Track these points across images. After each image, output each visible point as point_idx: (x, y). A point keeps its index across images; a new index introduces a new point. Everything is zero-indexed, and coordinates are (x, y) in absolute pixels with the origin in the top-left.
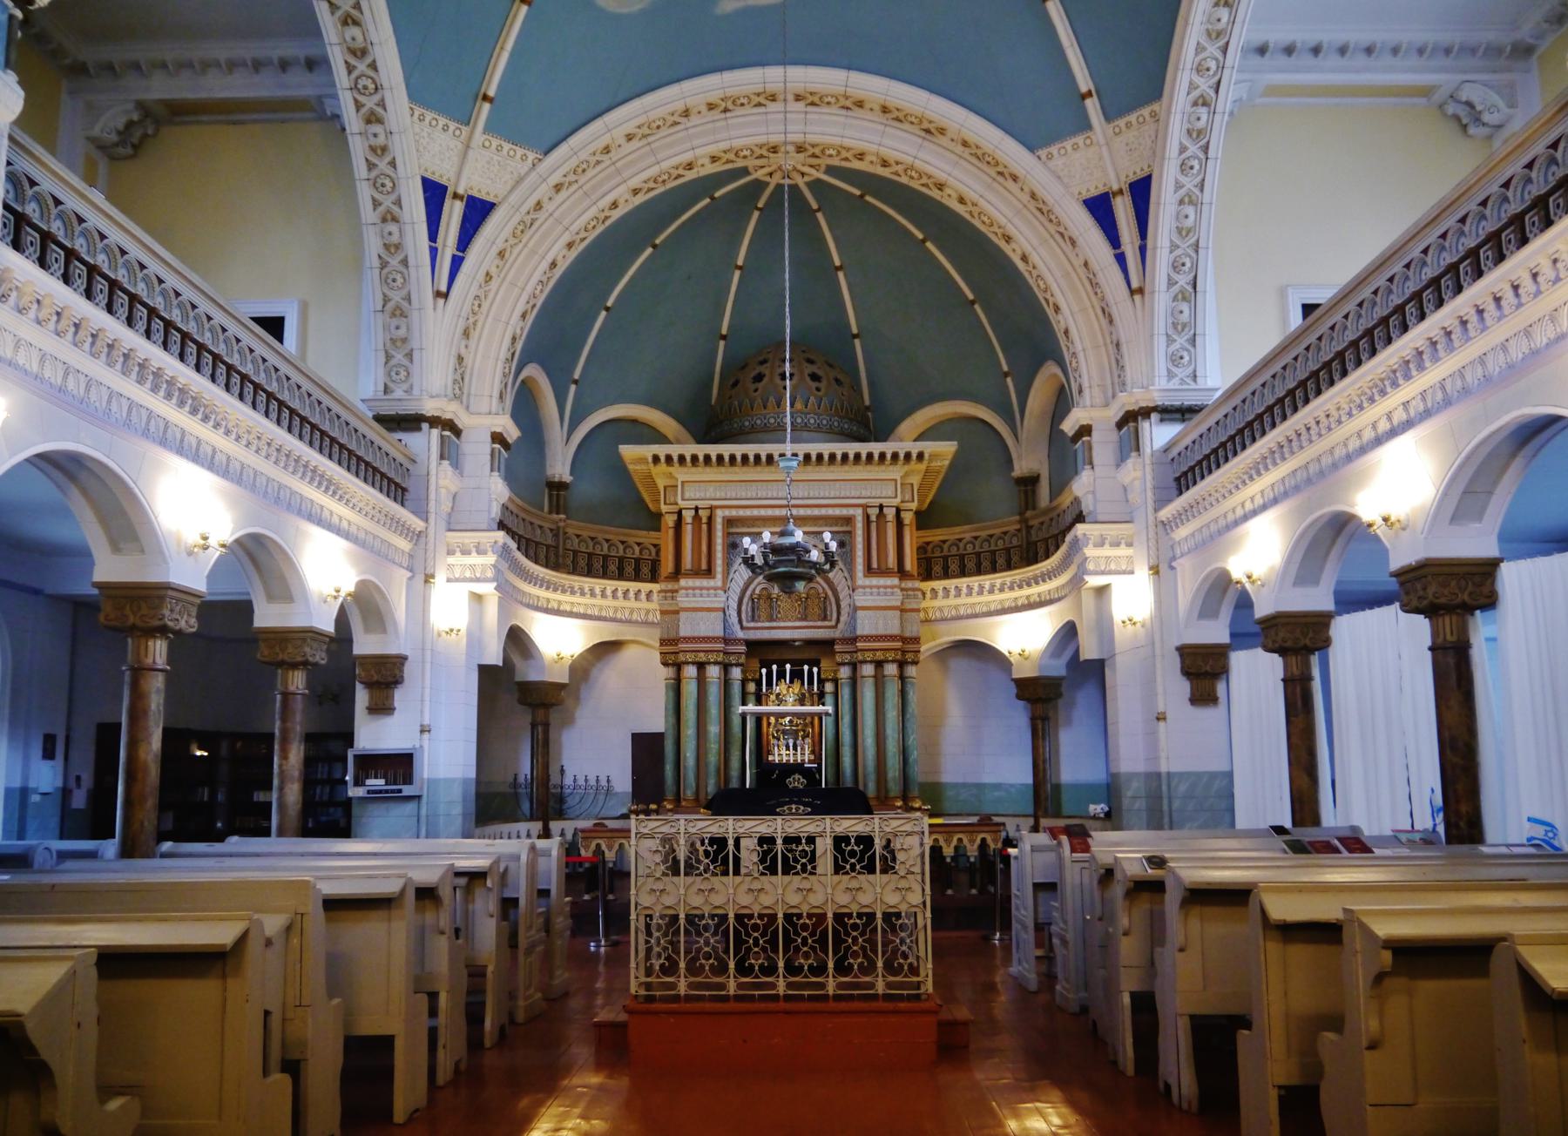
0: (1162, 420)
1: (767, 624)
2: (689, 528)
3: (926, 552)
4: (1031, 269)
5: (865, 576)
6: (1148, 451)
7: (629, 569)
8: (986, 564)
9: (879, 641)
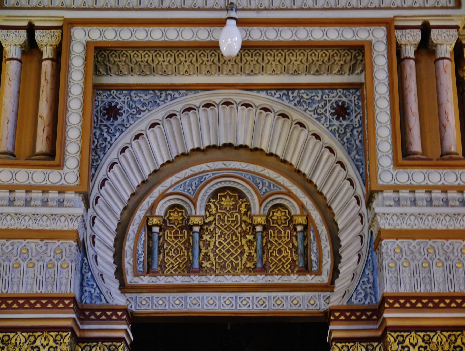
1: (179, 280)
5: (397, 165)
9: (436, 307)
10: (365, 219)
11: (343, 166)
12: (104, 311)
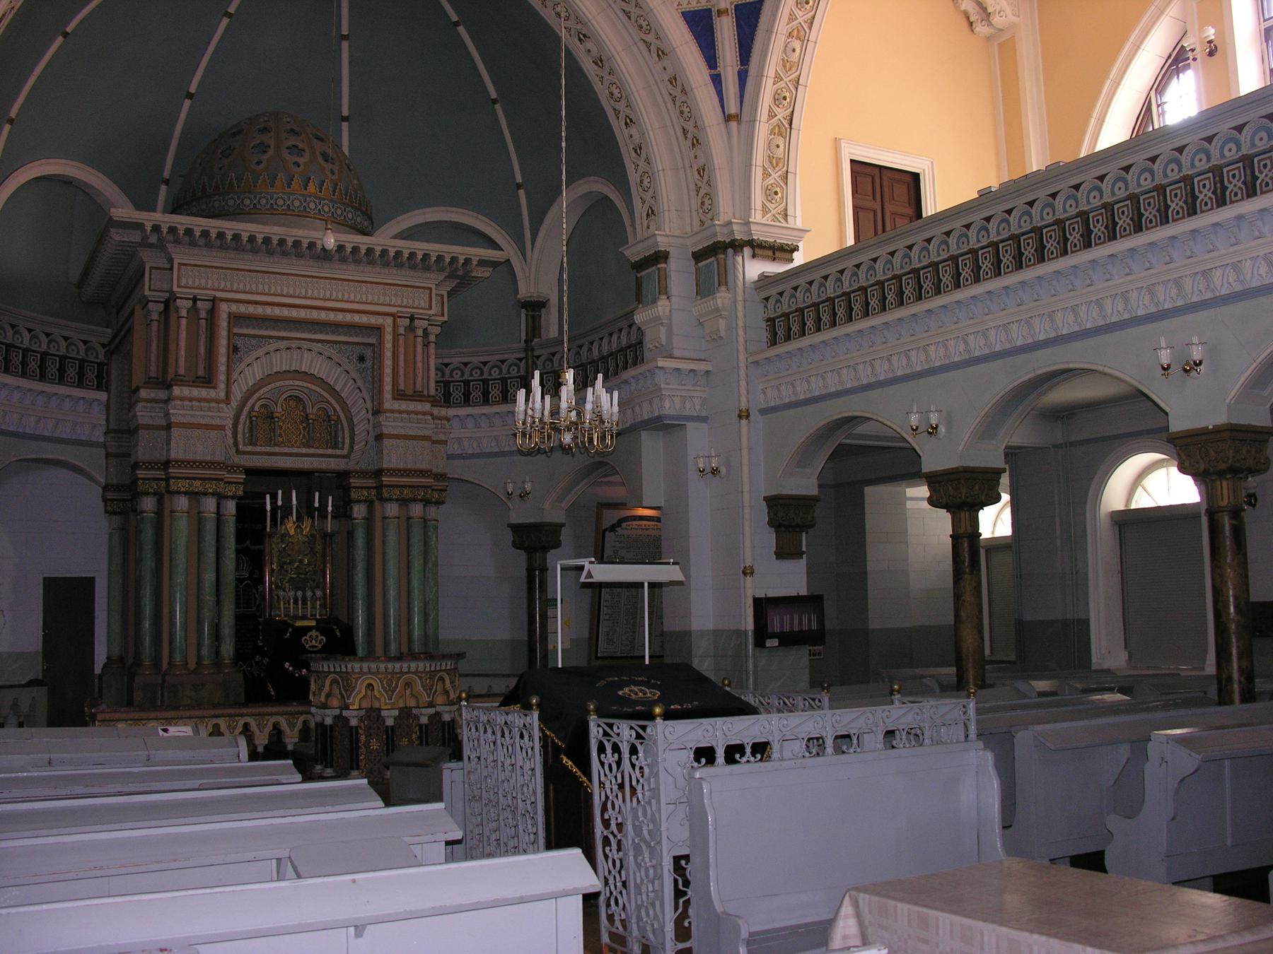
0: (754, 256)
1: (268, 449)
2: (184, 322)
3: (443, 375)
4: (605, 73)
6: (740, 284)
7: (53, 369)
8: (476, 394)
10: (371, 422)
11: (360, 390)
12: (232, 467)
